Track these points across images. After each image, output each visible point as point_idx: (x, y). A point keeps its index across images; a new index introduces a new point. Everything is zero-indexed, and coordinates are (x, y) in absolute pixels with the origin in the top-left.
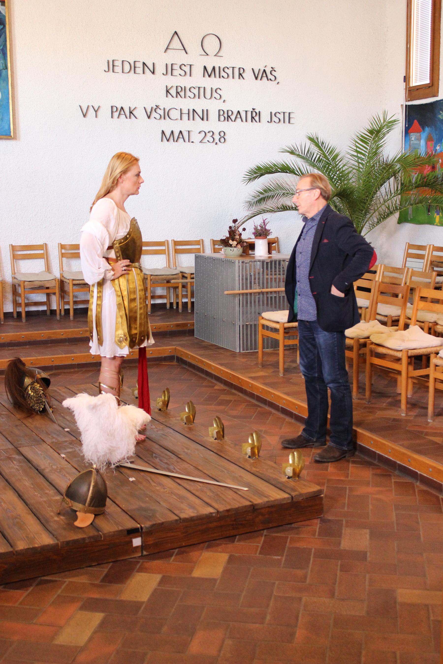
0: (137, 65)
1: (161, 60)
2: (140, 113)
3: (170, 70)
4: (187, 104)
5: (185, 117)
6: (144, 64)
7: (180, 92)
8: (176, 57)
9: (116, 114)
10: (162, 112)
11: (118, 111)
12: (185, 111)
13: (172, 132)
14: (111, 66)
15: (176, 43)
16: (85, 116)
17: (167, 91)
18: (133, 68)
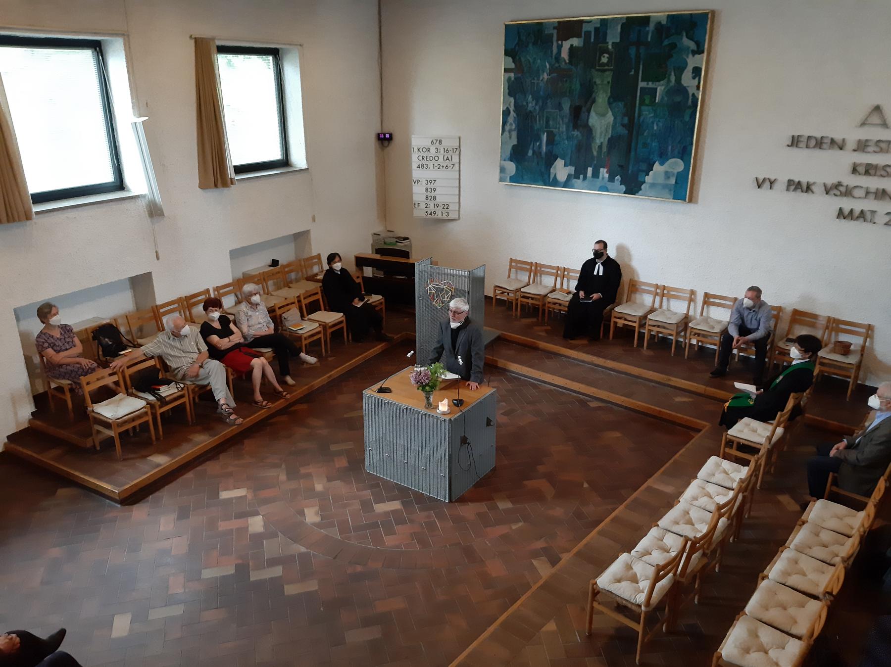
0: (825, 141)
1: (853, 136)
2: (818, 189)
3: (862, 146)
4: (874, 183)
5: (872, 196)
6: (833, 141)
7: (869, 170)
8: (875, 134)
9: (792, 187)
10: (843, 189)
11: (795, 186)
12: (873, 190)
13: (852, 211)
14: (795, 142)
15: (875, 119)
16: (759, 187)
17: (855, 170)
18: (819, 143)
